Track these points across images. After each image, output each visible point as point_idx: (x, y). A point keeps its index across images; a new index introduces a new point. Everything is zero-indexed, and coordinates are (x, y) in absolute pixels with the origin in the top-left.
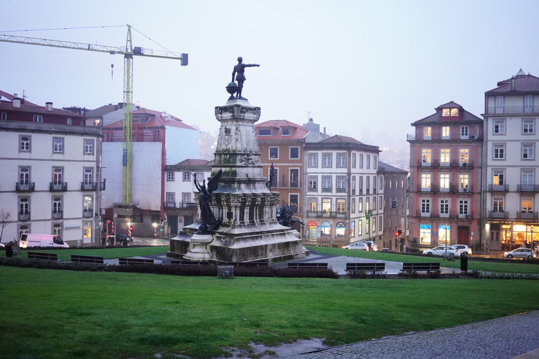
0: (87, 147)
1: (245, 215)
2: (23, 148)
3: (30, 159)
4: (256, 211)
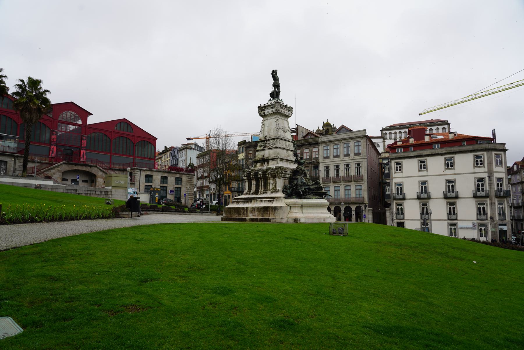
0: (477, 161)
1: (253, 186)
2: (421, 168)
3: (427, 176)
4: (262, 183)
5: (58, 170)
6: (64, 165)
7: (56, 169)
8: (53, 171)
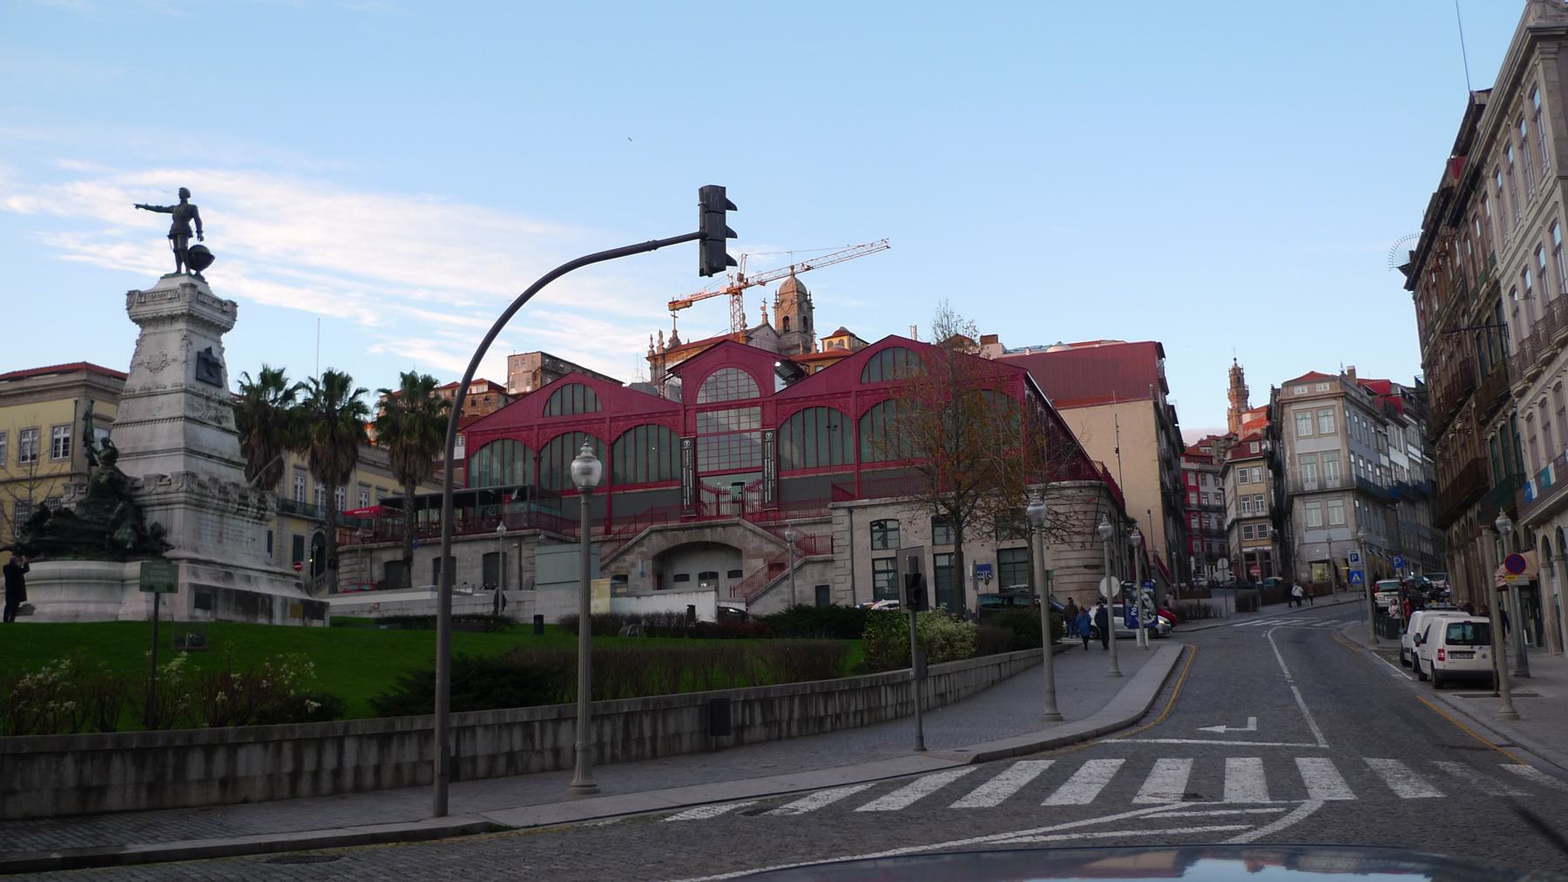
5: (642, 553)
6: (654, 536)
7: (637, 550)
8: (629, 558)
